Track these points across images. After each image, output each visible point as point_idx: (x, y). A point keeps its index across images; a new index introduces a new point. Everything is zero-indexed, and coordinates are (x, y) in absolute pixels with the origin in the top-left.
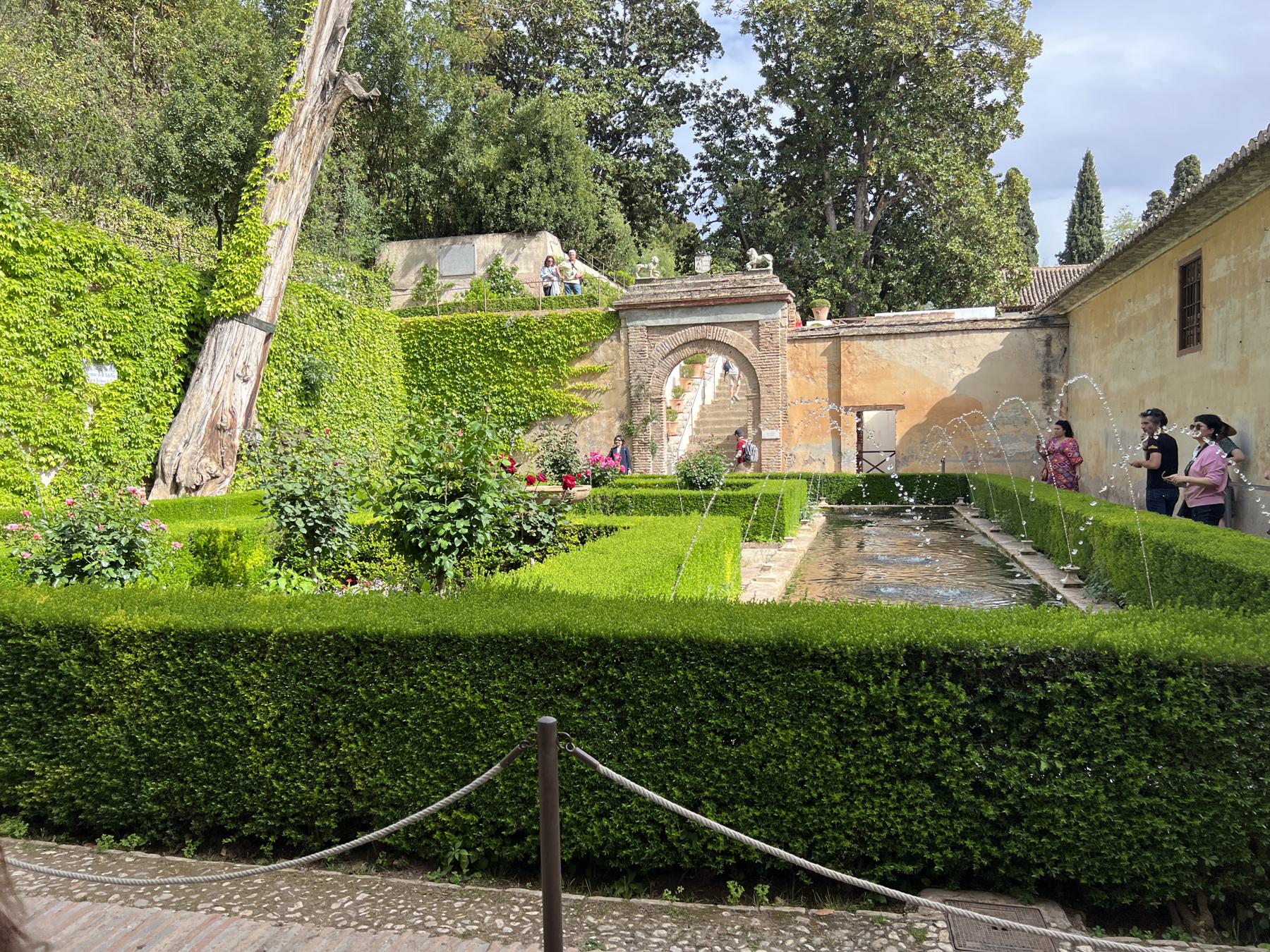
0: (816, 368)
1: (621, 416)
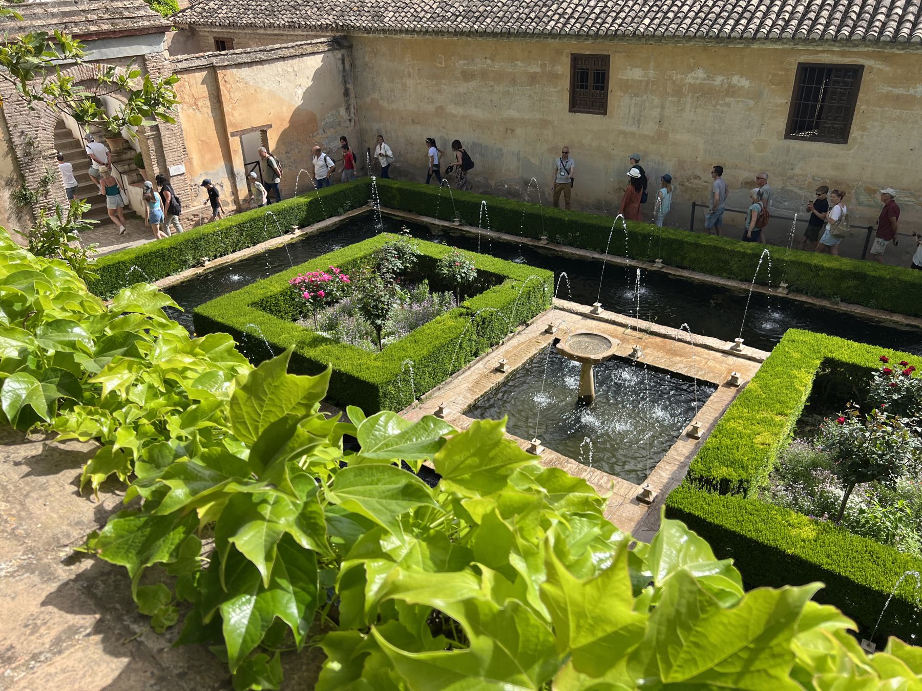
0: (199, 99)
1: (9, 183)
